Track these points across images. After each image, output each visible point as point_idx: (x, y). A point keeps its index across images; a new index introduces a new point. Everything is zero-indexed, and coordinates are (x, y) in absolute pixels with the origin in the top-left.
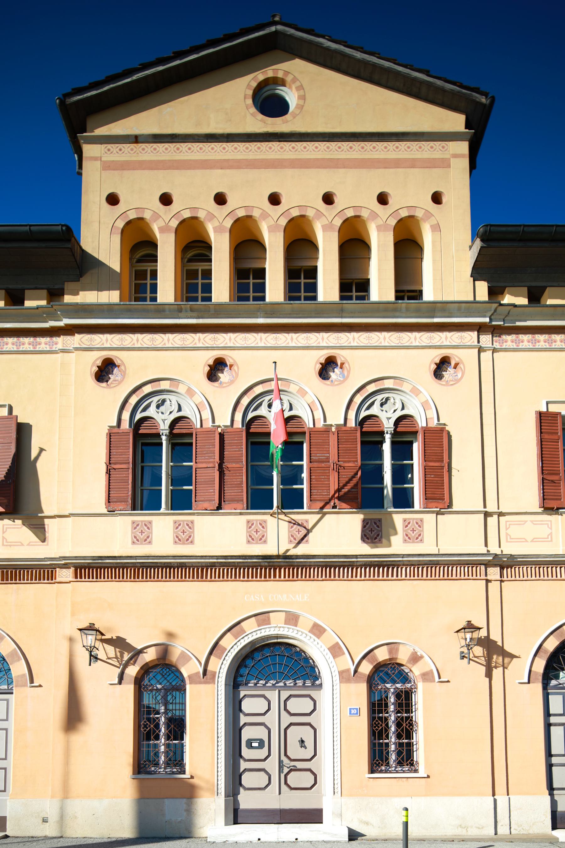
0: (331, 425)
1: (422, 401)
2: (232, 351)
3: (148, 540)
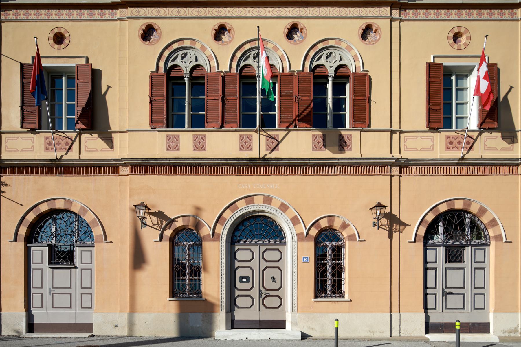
0: (294, 71)
1: (354, 55)
2: (230, 20)
3: (177, 148)
